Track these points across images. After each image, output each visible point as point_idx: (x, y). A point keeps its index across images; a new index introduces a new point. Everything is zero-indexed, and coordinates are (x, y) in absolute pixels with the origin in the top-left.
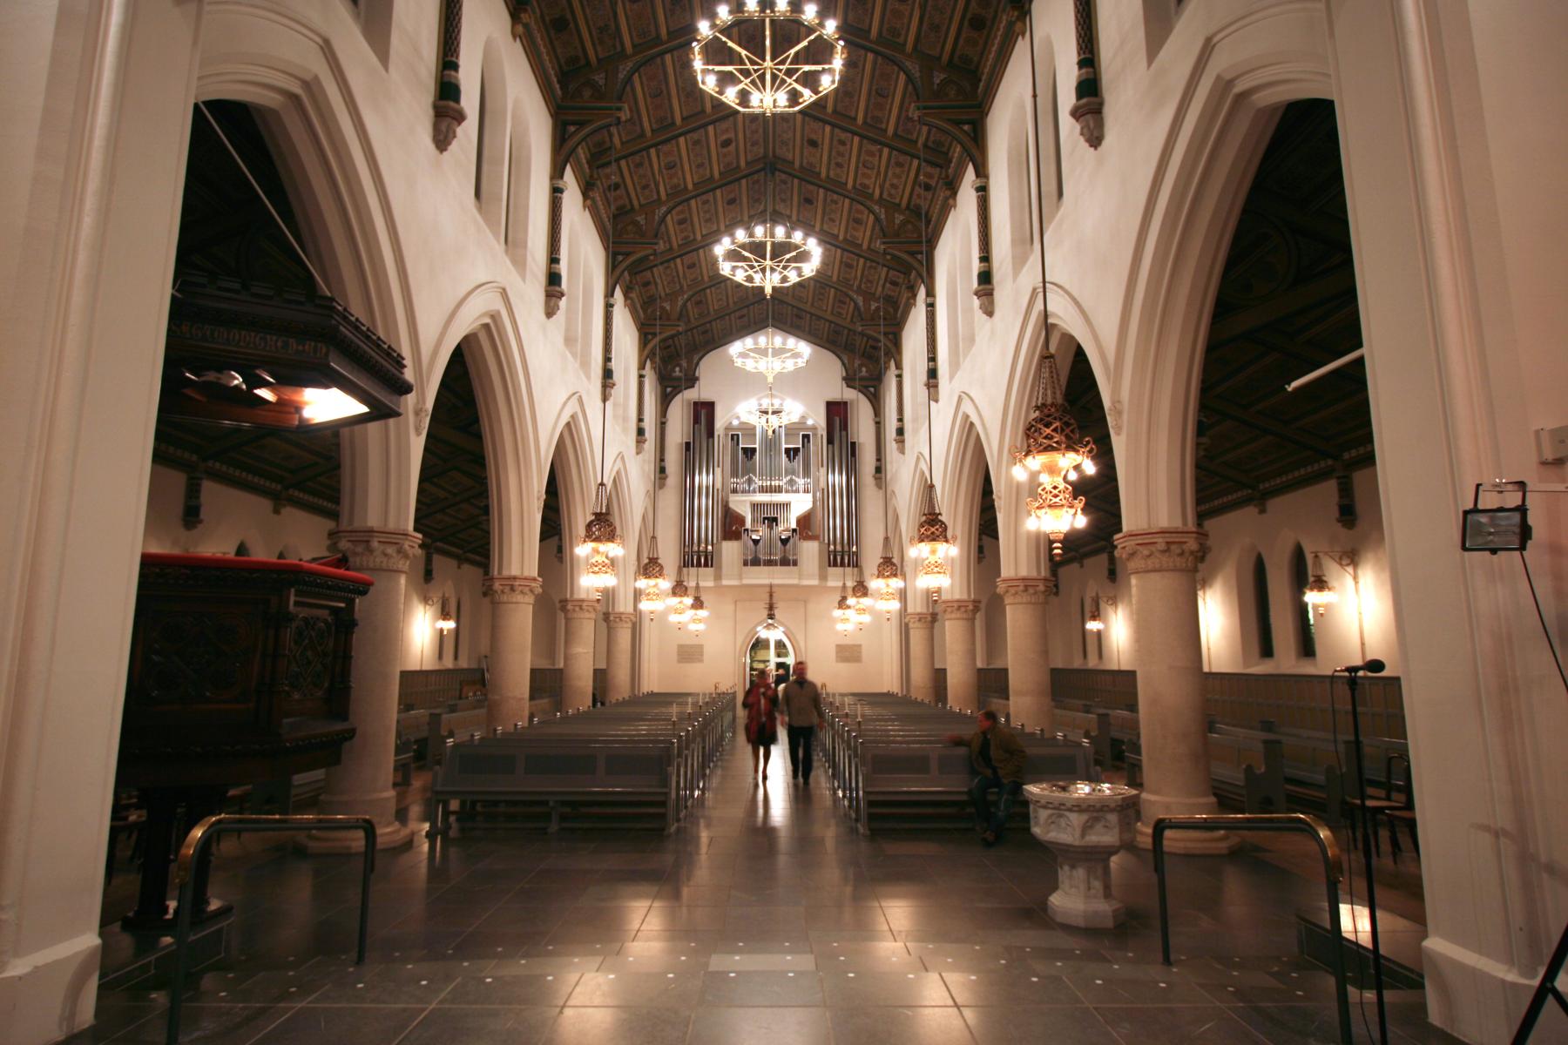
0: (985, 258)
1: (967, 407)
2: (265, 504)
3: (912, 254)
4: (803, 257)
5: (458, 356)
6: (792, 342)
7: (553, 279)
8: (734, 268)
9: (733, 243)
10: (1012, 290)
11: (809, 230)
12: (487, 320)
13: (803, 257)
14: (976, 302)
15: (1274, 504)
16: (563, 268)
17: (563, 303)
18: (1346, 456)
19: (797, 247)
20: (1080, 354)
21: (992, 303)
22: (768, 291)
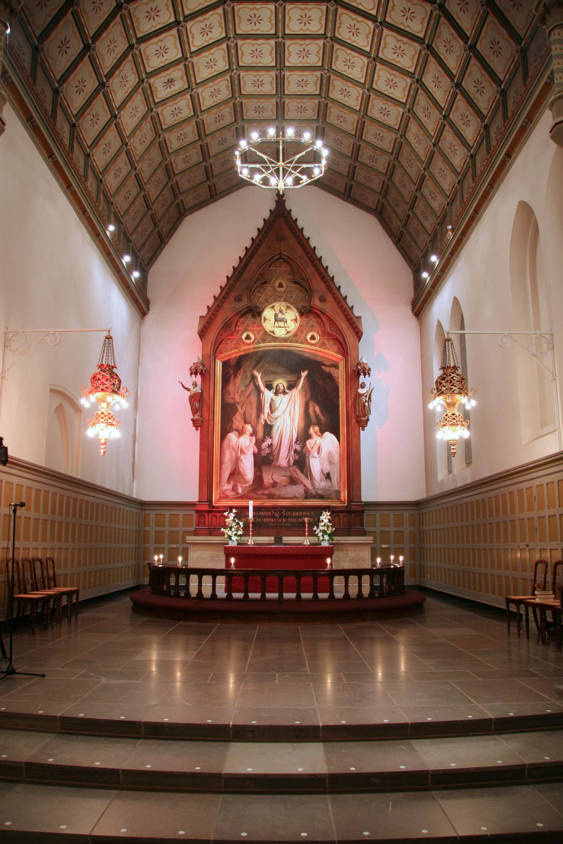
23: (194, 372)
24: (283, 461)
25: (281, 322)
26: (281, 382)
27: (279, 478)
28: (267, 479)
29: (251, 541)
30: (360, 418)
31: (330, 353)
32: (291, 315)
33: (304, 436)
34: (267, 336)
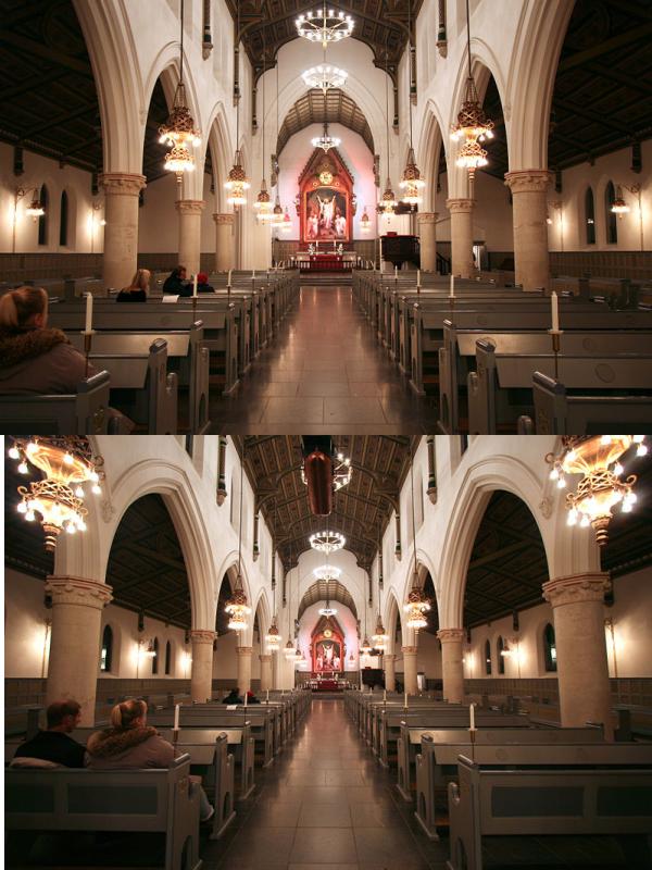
0: (443, 25)
1: (432, 108)
2: (56, 163)
3: (404, 22)
4: (344, 26)
5: (158, 80)
6: (336, 70)
7: (207, 38)
8: (306, 33)
9: (306, 18)
10: (456, 43)
11: (347, 12)
12: (173, 63)
13: (344, 26)
14: (437, 50)
15: (598, 161)
16: (212, 32)
17: (212, 51)
18: (637, 134)
19: (339, 21)
20: (492, 78)
21: (446, 50)
22: (325, 44)
23: (297, 197)
24: (327, 227)
25: (326, 178)
26: (326, 200)
27: (326, 232)
28: (322, 232)
29: (317, 253)
30: (353, 212)
31: (343, 190)
32: (330, 176)
33: (334, 218)
34: (321, 184)
